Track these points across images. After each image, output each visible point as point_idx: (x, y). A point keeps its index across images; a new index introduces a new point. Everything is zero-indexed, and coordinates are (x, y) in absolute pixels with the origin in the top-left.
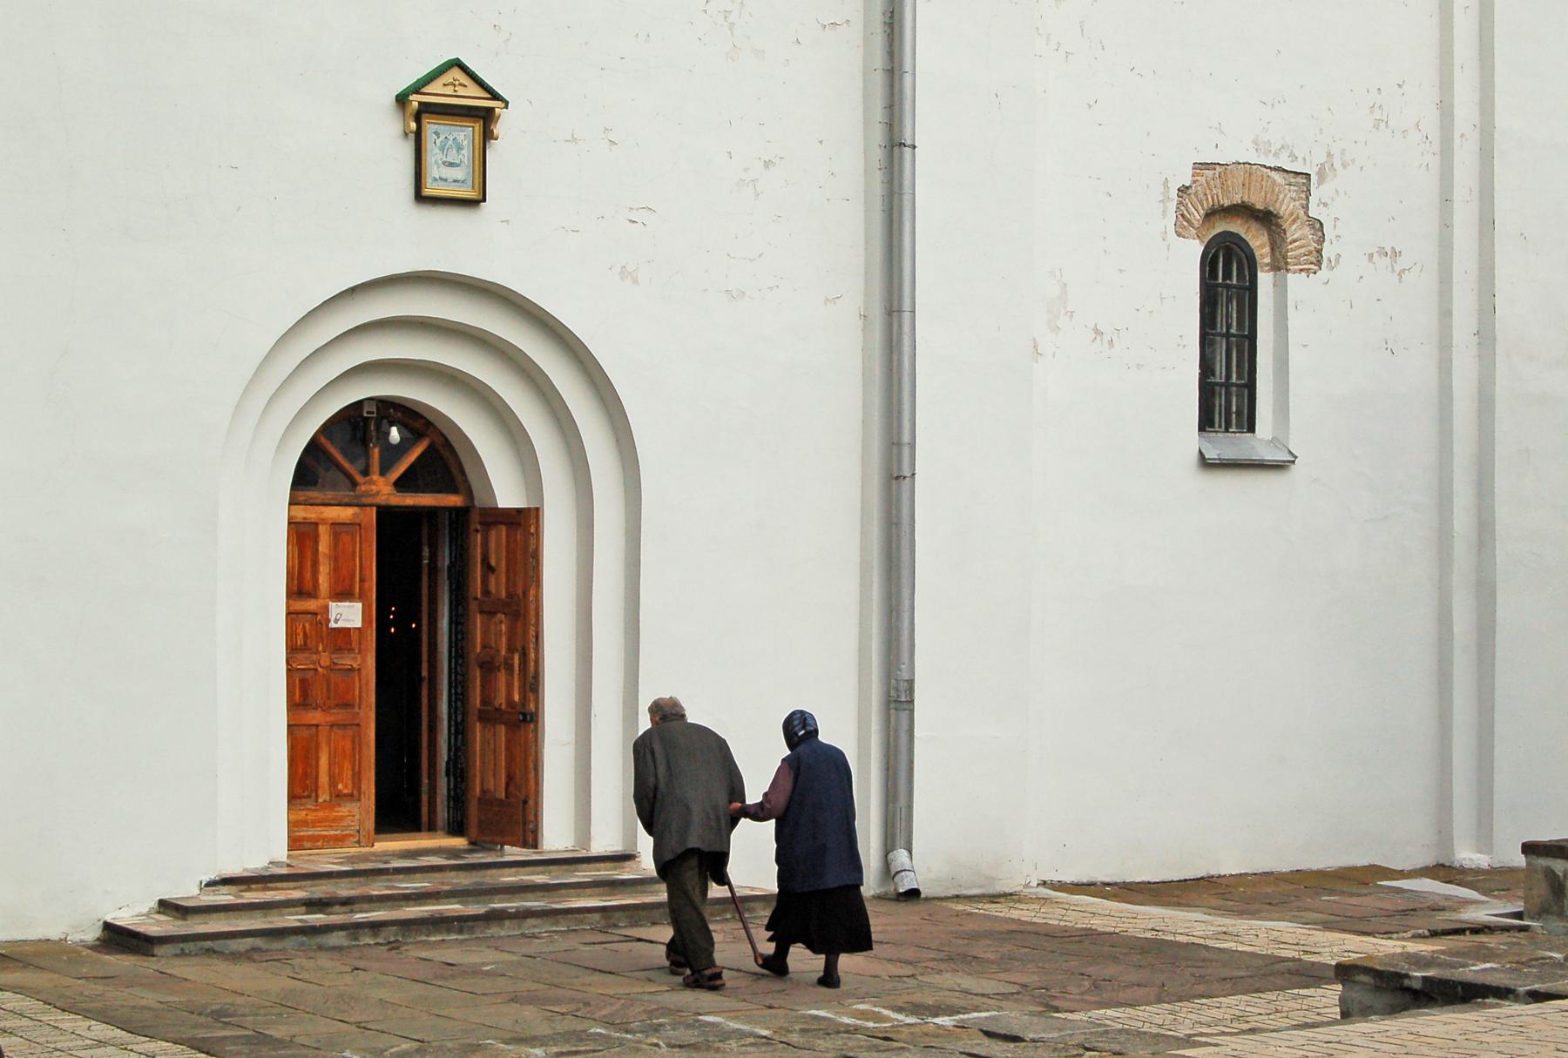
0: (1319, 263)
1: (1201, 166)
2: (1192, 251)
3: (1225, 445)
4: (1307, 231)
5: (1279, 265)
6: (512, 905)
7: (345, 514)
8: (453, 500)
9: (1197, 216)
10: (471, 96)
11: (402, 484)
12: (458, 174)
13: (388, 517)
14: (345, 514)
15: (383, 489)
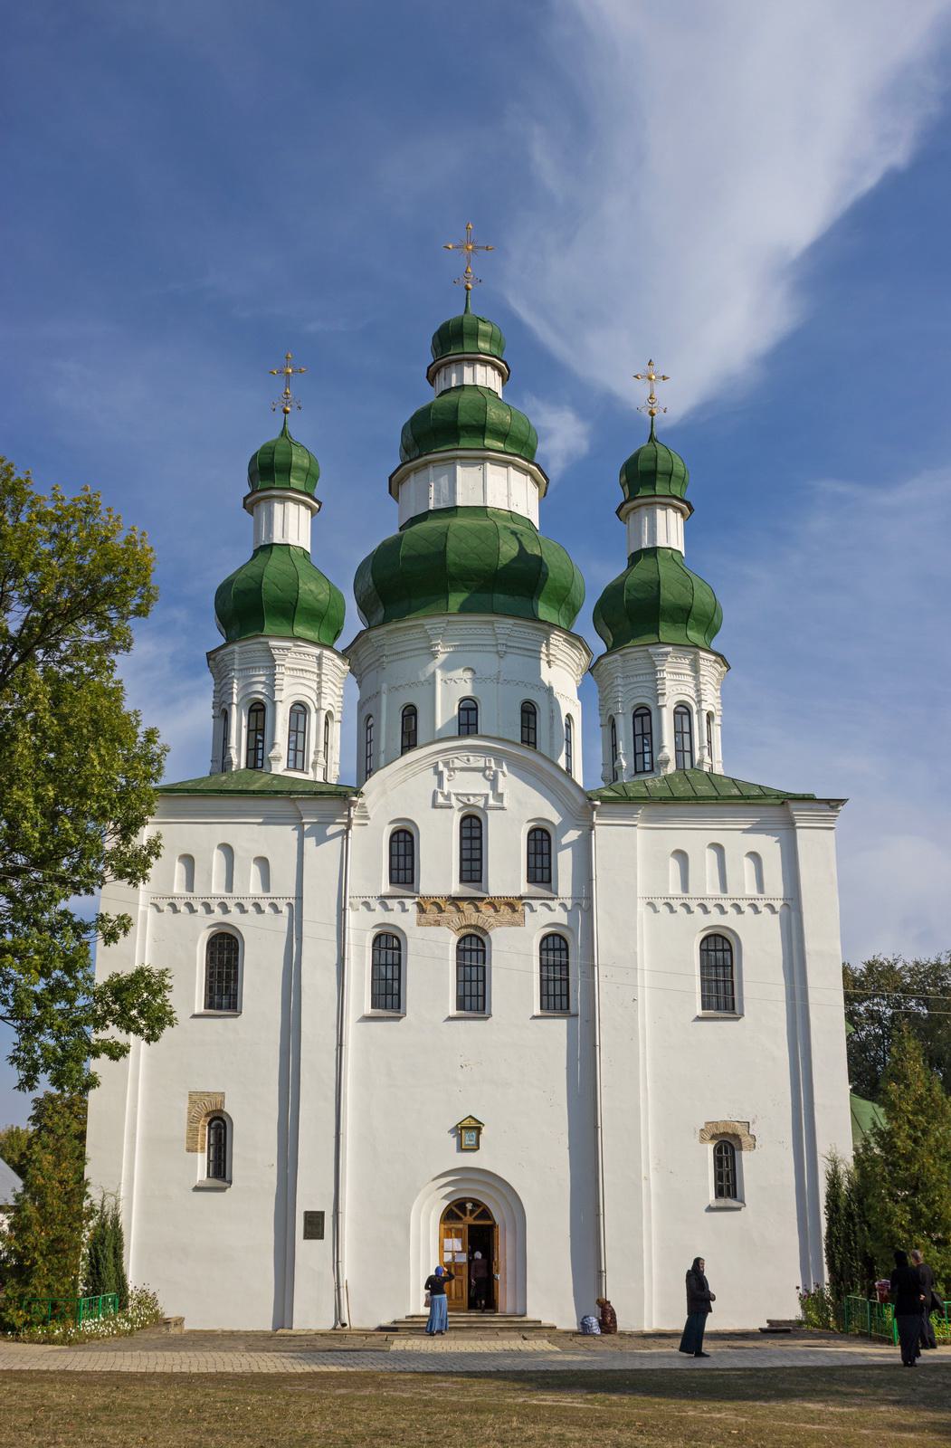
0: (755, 1147)
1: (707, 1123)
2: (710, 1147)
3: (724, 1202)
4: (749, 1138)
5: (741, 1149)
6: (487, 1325)
7: (461, 1226)
8: (489, 1222)
9: (708, 1137)
10: (473, 1124)
11: (475, 1219)
12: (473, 1143)
13: (470, 1227)
14: (461, 1226)
15: (469, 1220)
